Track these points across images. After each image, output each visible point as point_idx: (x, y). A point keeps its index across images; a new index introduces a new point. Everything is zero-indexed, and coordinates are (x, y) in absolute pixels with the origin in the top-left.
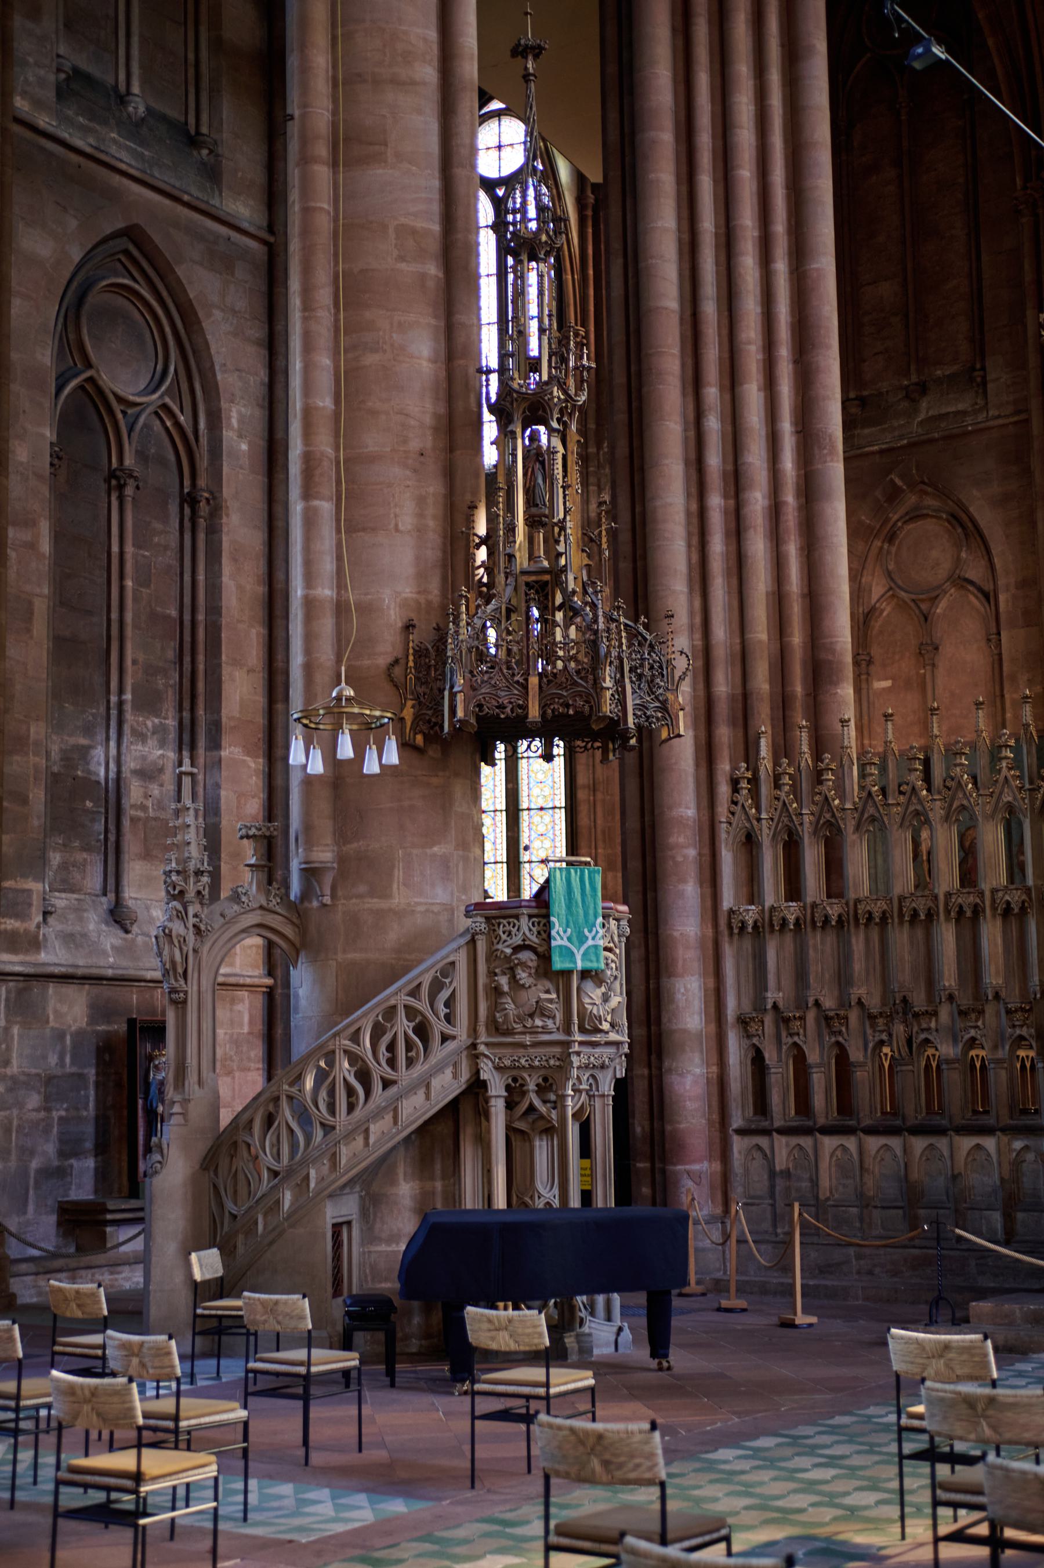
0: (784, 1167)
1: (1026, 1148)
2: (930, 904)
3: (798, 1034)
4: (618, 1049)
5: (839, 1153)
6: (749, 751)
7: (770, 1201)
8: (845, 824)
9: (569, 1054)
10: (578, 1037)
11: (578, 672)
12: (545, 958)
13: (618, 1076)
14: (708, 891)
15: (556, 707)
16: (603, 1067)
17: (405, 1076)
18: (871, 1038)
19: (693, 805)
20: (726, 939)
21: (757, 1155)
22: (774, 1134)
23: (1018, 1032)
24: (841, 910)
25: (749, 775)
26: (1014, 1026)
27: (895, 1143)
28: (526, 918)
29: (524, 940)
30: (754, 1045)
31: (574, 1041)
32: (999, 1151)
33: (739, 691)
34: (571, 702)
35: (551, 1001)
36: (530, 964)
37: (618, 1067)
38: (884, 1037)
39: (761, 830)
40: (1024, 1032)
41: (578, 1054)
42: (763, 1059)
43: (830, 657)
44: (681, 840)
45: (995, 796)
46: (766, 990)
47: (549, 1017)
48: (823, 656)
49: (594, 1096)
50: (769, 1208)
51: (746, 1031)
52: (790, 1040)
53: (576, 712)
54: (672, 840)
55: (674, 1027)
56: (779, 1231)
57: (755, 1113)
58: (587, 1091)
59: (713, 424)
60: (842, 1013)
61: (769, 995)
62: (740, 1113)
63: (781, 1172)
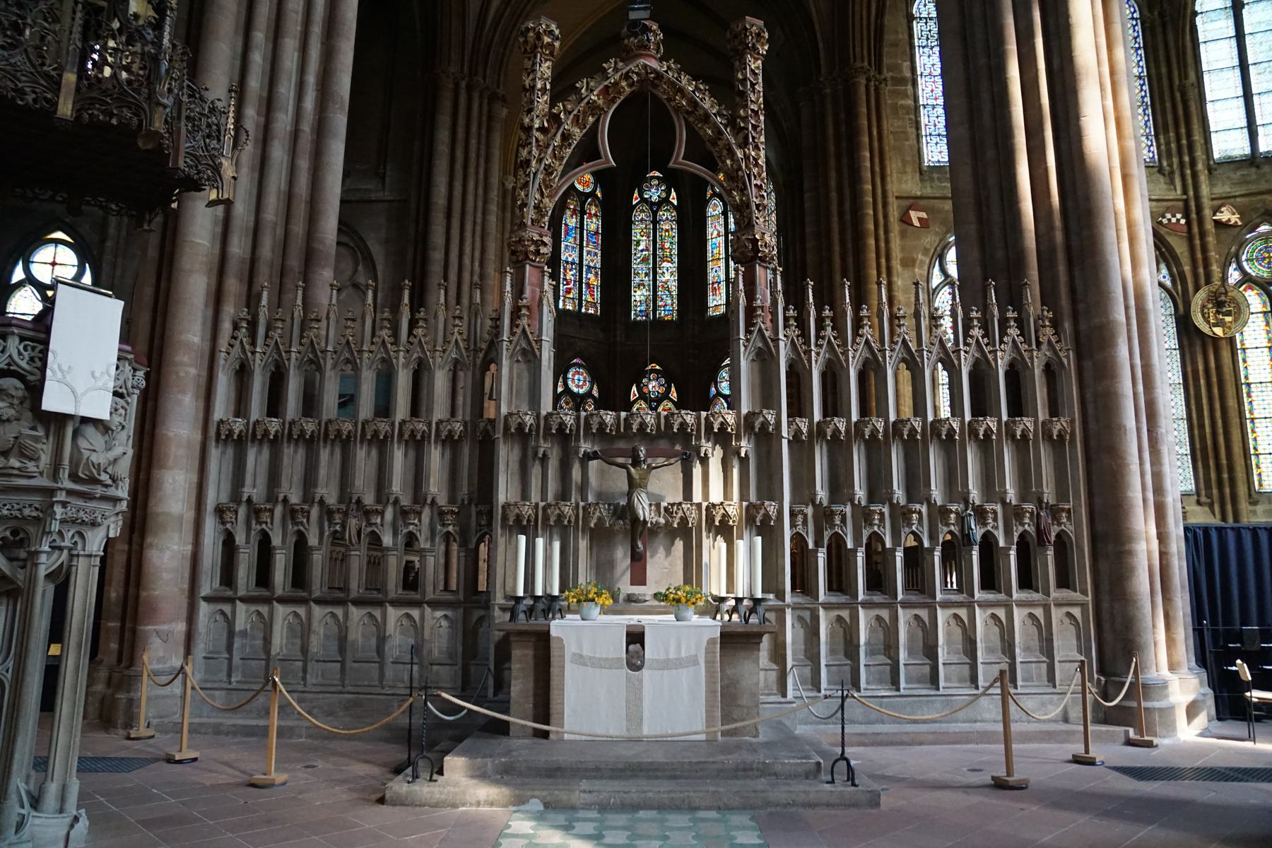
0: (242, 628)
1: (446, 617)
2: (387, 428)
3: (266, 523)
4: (115, 506)
5: (291, 618)
6: (251, 300)
7: (227, 656)
8: (325, 363)
9: (52, 505)
10: (69, 485)
11: (129, 82)
12: (35, 390)
13: (111, 535)
14: (201, 405)
15: (96, 113)
16: (94, 524)
18: (327, 528)
19: (199, 334)
20: (213, 444)
21: (218, 617)
22: (238, 602)
24: (313, 428)
25: (249, 317)
28: (17, 340)
29: (9, 364)
30: (227, 530)
31: (61, 489)
32: (422, 617)
33: (248, 256)
34: (115, 112)
35: (37, 439)
36: (13, 392)
37: (112, 526)
38: (338, 528)
39: (254, 361)
41: (64, 504)
42: (234, 541)
43: (321, 247)
44: (186, 359)
45: (447, 353)
46: (243, 485)
47: (31, 459)
48: (316, 245)
49: (78, 556)
50: (226, 661)
51: (221, 518)
52: (259, 527)
53: (120, 122)
54: (178, 359)
55: (160, 510)
56: (233, 680)
57: (221, 585)
58: (70, 549)
59: (258, 58)
60: (306, 507)
61: (245, 489)
62: (208, 584)
63: (240, 631)
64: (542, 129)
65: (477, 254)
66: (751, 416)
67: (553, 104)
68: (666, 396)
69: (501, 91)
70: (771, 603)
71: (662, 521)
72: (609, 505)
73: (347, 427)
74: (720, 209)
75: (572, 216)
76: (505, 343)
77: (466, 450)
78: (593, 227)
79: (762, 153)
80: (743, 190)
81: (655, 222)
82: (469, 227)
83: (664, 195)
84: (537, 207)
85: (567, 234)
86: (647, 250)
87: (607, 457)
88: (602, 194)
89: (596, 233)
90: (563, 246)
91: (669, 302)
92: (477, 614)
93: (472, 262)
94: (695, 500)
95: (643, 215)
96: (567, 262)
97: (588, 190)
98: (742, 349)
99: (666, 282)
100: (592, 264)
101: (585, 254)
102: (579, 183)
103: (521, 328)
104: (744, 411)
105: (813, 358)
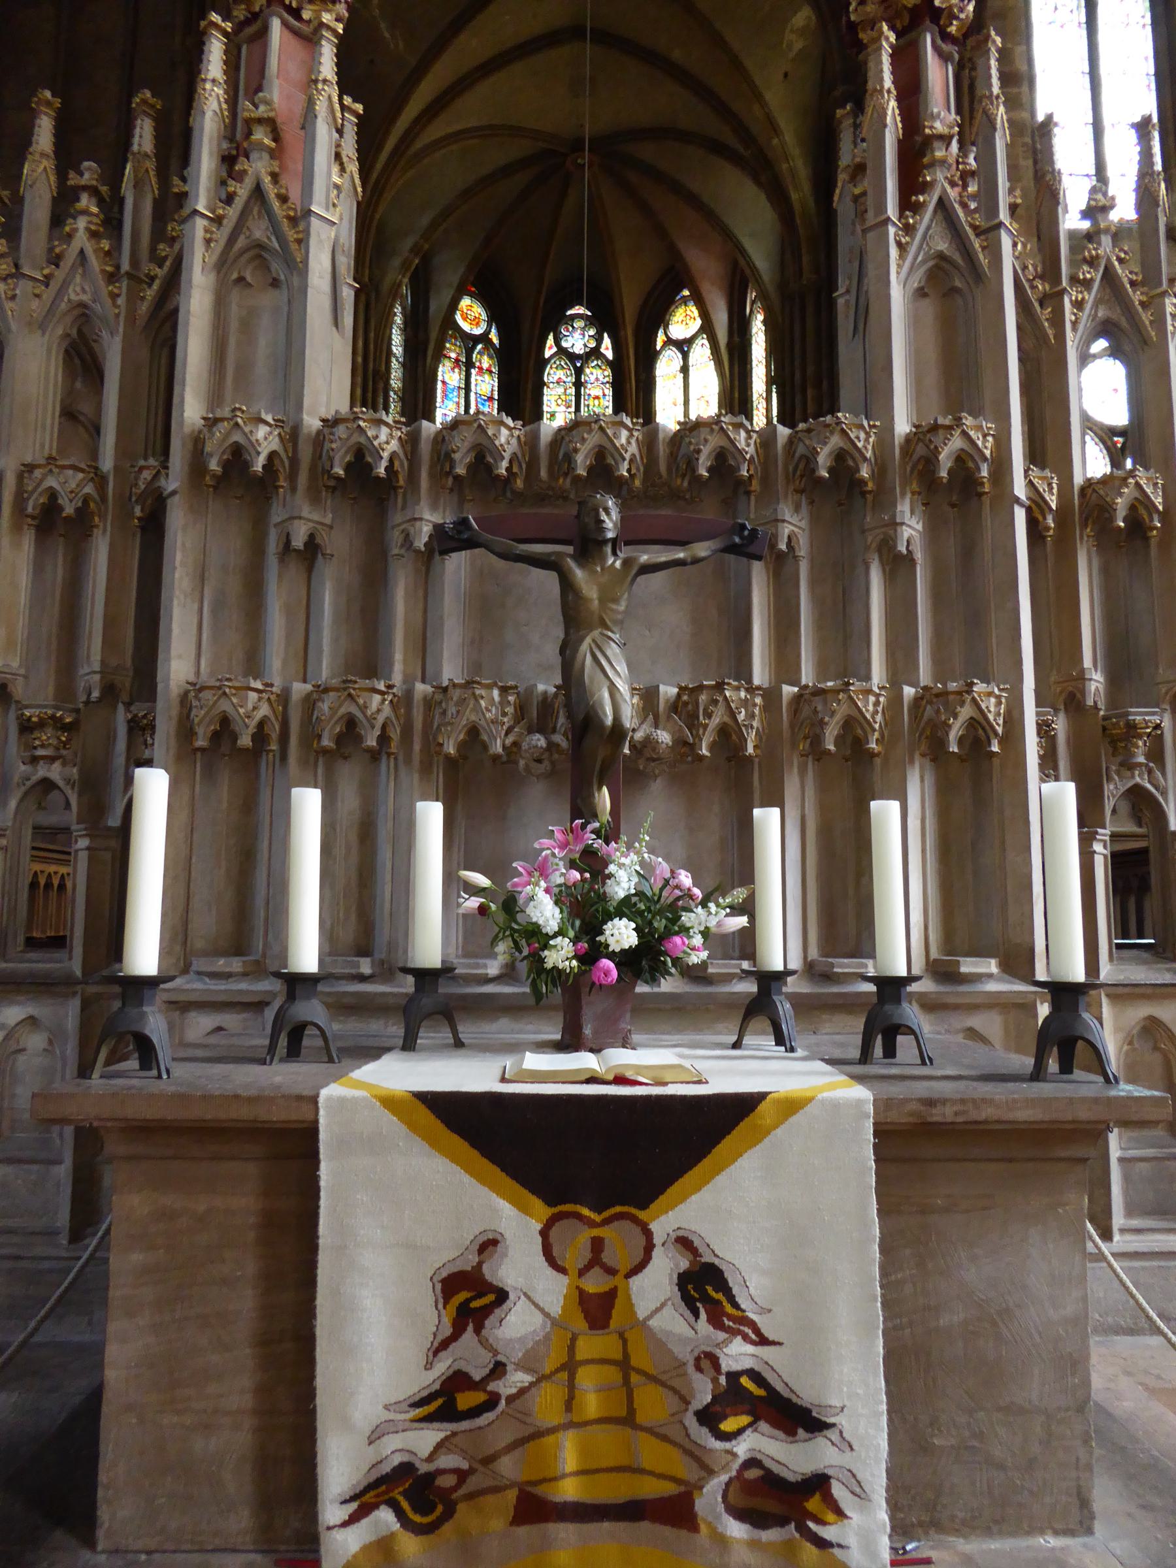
1: (32, 1021)
23: (42, 771)
26: (34, 760)
40: (55, 772)
45: (55, 285)
70: (992, 987)
71: (664, 737)
72: (504, 690)
75: (453, 369)
76: (200, 223)
81: (578, 385)
83: (593, 344)
85: (445, 396)
88: (500, 339)
89: (491, 399)
94: (757, 681)
95: (560, 374)
97: (478, 331)
98: (894, 252)
102: (465, 319)
103: (249, 182)
105: (1069, 317)
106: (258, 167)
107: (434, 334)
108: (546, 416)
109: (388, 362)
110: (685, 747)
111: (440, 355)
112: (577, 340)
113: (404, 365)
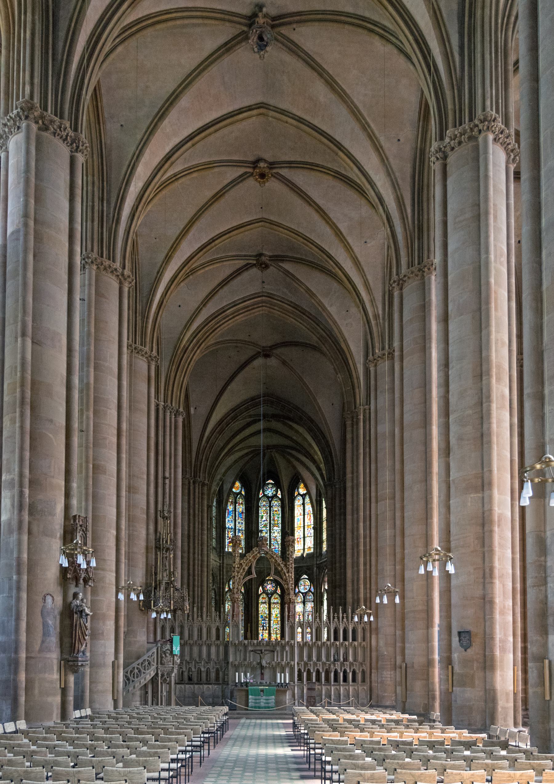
17: (147, 672)
27: (192, 686)
64: (238, 568)
65: (200, 552)
66: (288, 641)
67: (240, 560)
68: (275, 592)
69: (206, 482)
73: (192, 642)
74: (301, 502)
77: (221, 649)
78: (241, 510)
79: (293, 574)
80: (288, 584)
81: (270, 507)
82: (197, 542)
84: (237, 588)
85: (228, 514)
86: (266, 520)
87: (254, 651)
89: (242, 513)
90: (227, 520)
91: (277, 547)
92: (224, 687)
93: (198, 555)
96: (229, 528)
99: (275, 537)
100: (240, 528)
101: (237, 523)
104: (287, 640)
106: (235, 618)
107: (225, 497)
108: (260, 517)
109: (216, 526)
110: (269, 667)
111: (227, 501)
112: (270, 492)
113: (216, 507)
